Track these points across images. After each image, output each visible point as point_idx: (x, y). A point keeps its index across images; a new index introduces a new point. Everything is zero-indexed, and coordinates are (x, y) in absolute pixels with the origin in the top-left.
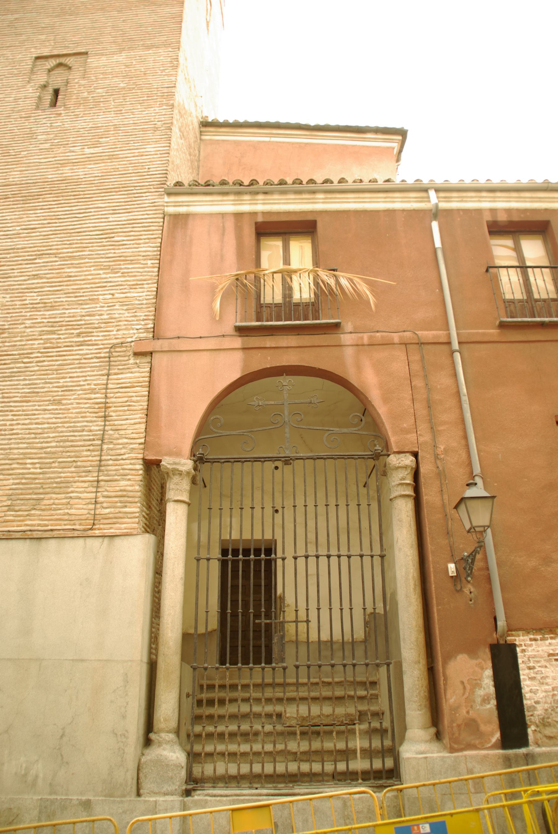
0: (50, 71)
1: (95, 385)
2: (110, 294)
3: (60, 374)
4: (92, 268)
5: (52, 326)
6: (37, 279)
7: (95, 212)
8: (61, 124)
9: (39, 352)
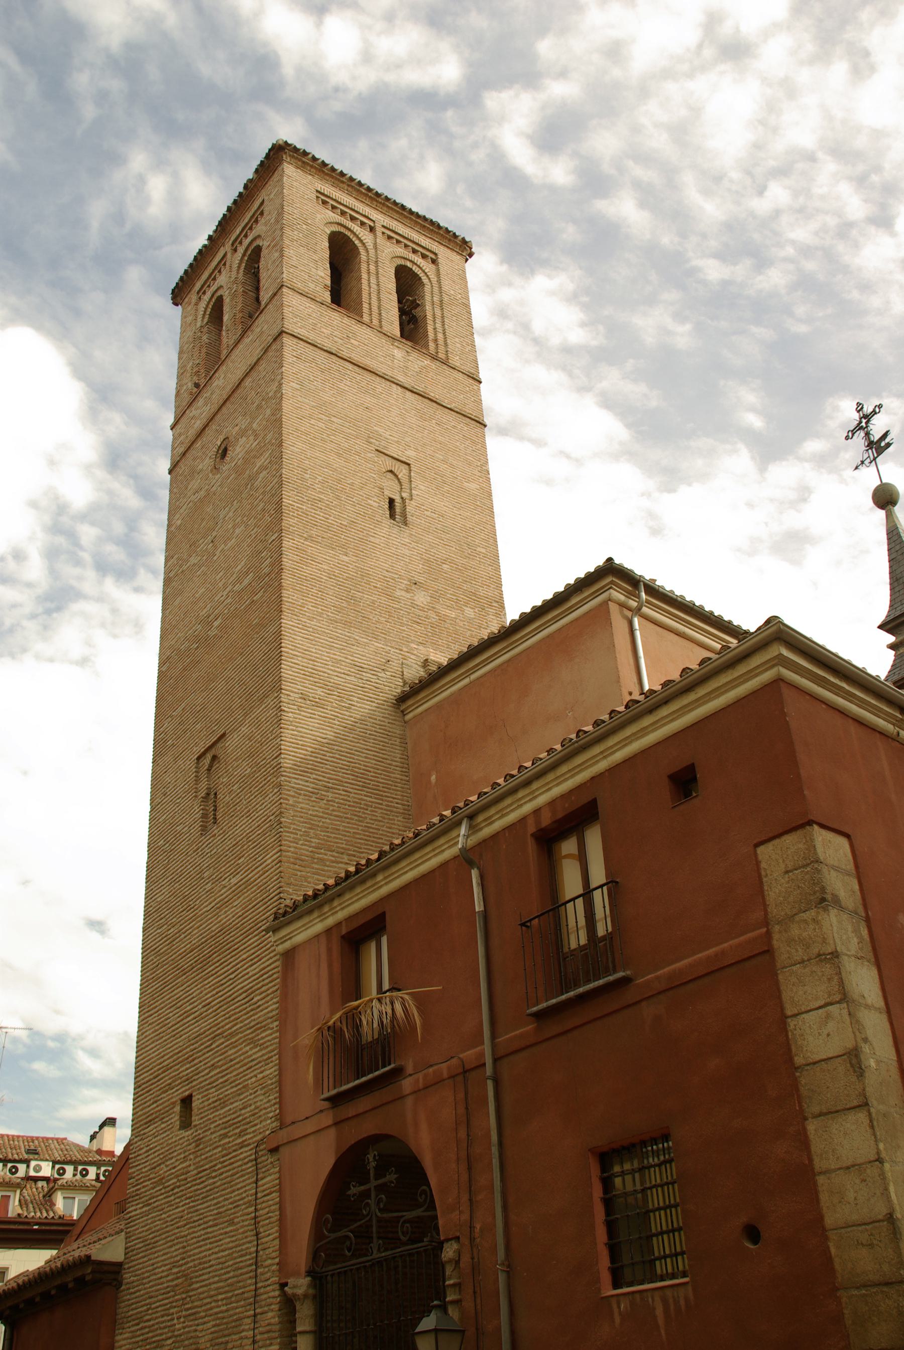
0: (209, 770)
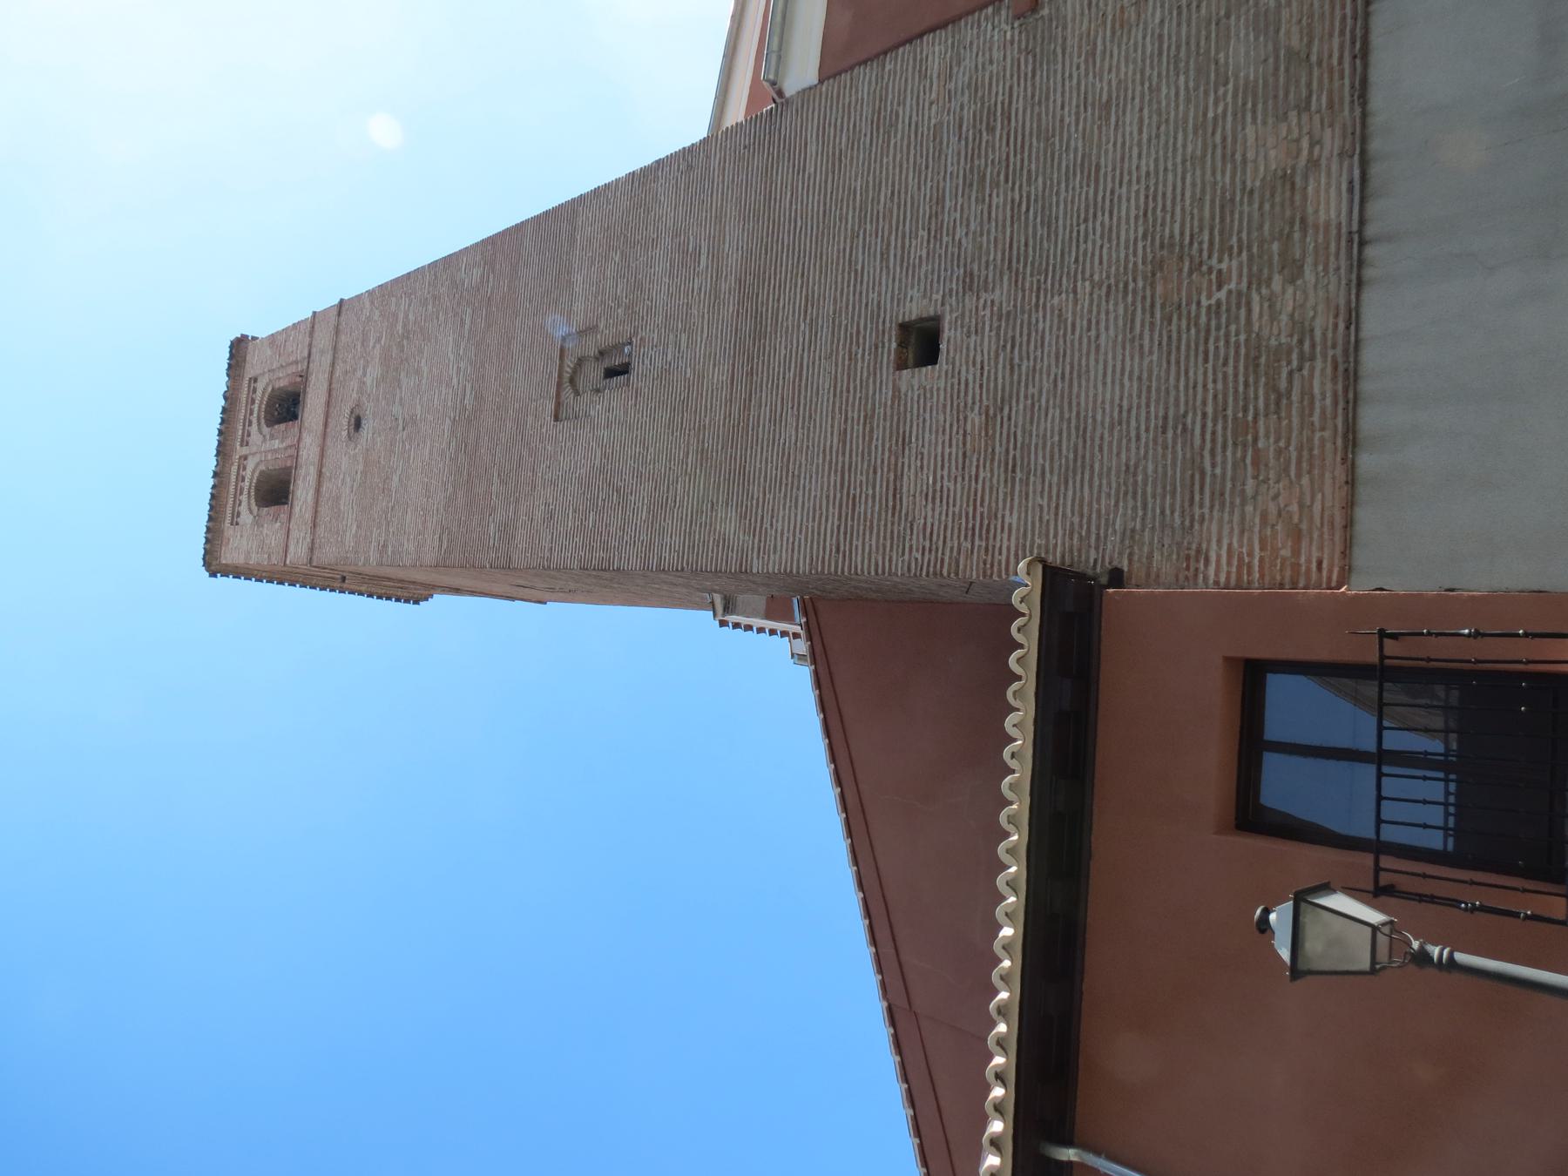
0: (577, 393)
1: (1079, 57)
2: (930, 109)
3: (1054, 130)
5: (971, 185)
6: (888, 257)
9: (1013, 189)
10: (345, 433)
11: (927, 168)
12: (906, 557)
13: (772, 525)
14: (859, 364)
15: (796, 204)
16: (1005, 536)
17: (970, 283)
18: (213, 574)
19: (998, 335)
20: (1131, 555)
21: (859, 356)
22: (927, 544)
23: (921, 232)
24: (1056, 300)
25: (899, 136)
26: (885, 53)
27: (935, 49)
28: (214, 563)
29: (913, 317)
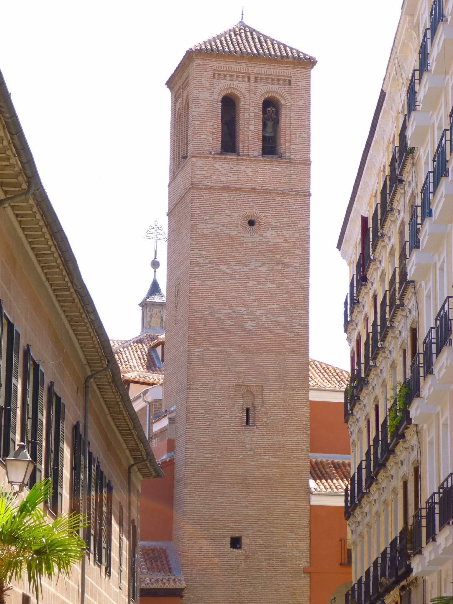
4: (283, 529)
5: (269, 556)
7: (280, 498)
8: (256, 439)
10: (248, 212)
11: (277, 543)
12: (187, 542)
13: (196, 495)
14: (234, 524)
15: (280, 498)
16: (191, 570)
17: (247, 557)
18: (188, 52)
19: (234, 566)
20: (186, 600)
21: (236, 524)
22: (190, 548)
23: (262, 542)
24: (239, 580)
25: (287, 534)
26: (310, 528)
27: (305, 545)
28: (194, 54)
29: (242, 541)
